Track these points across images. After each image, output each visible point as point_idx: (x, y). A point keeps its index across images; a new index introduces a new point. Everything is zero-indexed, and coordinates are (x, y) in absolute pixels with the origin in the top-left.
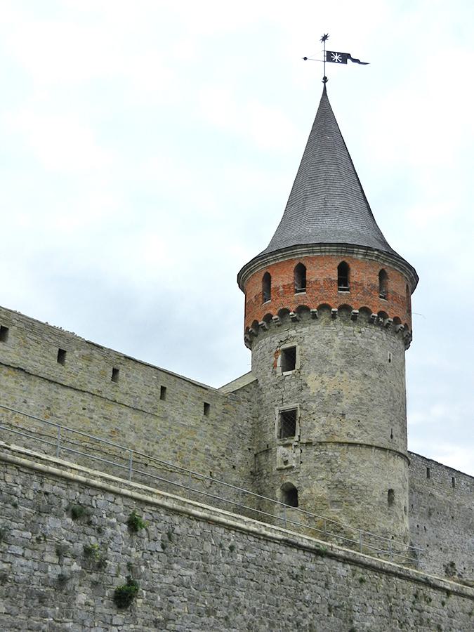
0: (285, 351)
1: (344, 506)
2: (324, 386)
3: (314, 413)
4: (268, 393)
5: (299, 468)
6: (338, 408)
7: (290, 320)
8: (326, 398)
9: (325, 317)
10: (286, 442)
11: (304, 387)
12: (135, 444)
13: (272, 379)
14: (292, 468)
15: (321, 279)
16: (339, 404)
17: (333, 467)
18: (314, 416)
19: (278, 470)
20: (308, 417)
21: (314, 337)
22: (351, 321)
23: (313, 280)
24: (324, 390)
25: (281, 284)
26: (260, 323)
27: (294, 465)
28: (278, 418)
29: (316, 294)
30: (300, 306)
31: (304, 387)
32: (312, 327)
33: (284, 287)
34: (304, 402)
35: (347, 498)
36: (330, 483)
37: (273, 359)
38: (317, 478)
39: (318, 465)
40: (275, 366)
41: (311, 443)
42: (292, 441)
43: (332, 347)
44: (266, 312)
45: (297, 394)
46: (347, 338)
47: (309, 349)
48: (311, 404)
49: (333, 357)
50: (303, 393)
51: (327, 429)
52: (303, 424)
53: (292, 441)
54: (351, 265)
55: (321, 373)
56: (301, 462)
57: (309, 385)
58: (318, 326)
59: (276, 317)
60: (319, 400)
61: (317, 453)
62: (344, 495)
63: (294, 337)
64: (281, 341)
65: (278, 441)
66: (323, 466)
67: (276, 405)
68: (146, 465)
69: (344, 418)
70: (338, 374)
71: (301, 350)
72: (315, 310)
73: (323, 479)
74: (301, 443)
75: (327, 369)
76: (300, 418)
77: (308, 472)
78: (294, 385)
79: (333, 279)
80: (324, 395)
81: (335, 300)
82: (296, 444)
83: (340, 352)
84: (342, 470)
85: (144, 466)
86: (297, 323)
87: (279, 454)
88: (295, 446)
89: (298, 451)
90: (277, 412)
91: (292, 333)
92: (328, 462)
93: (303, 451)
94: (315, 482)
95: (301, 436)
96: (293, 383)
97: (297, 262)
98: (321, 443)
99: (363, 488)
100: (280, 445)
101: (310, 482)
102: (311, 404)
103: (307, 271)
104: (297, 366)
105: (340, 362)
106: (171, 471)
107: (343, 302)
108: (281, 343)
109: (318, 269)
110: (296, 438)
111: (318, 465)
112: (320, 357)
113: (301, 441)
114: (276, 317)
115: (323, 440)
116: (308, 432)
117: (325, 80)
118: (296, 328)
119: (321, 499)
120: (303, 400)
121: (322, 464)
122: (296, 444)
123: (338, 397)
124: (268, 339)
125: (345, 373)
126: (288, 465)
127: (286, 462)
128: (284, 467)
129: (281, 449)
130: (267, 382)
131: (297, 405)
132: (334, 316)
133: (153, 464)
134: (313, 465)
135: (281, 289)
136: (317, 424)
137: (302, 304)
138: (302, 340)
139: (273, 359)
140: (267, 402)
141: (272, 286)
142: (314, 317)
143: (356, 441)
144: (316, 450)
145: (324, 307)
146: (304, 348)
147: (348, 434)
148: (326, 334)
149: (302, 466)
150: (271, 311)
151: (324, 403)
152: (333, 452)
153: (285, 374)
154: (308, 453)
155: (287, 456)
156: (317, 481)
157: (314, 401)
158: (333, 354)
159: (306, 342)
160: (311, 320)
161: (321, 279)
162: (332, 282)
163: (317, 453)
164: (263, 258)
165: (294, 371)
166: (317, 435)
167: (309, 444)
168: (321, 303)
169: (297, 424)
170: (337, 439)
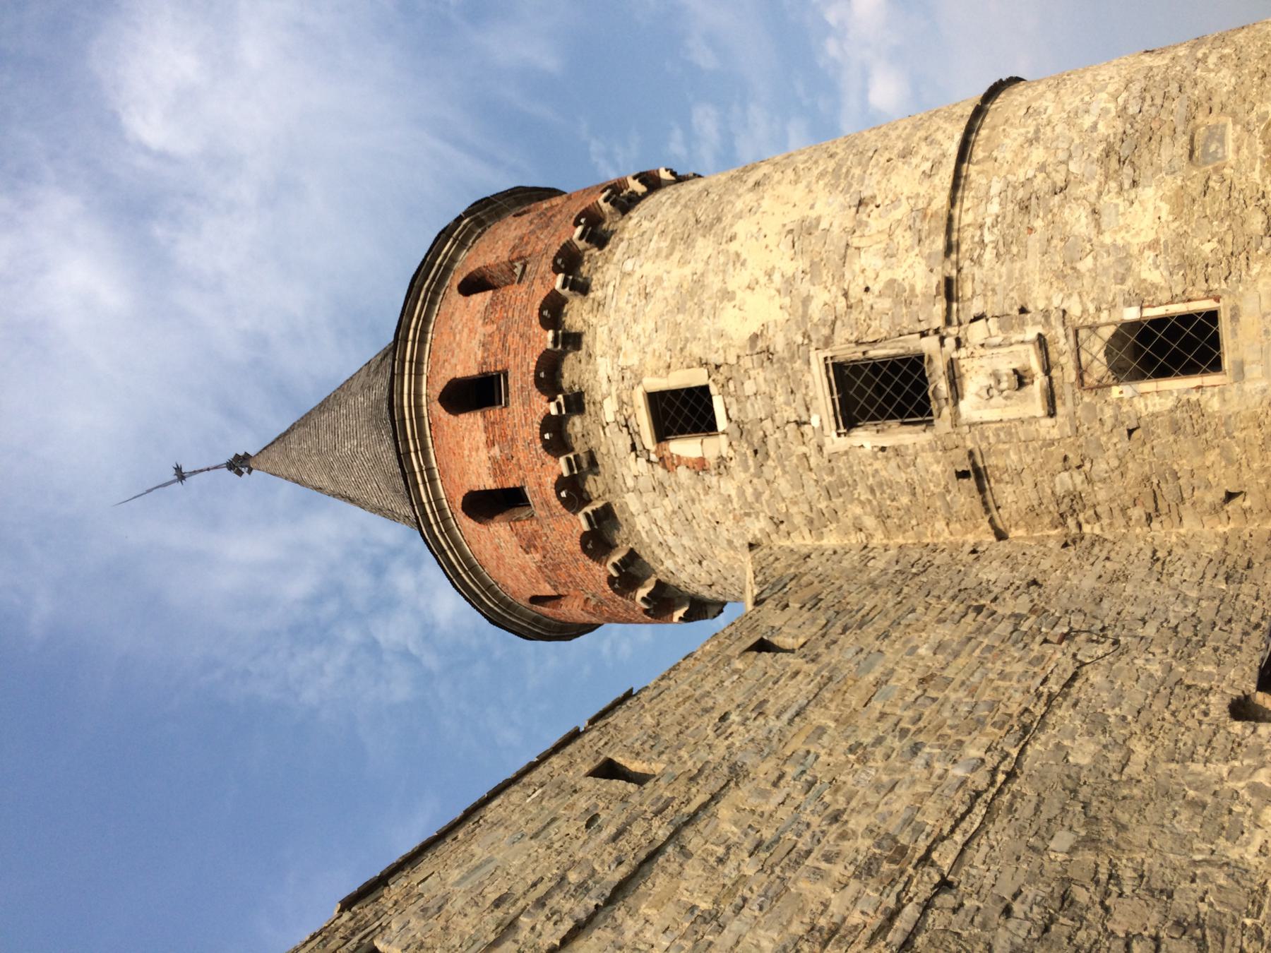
0: (662, 434)
1: (1212, 120)
2: (763, 280)
3: (846, 295)
4: (783, 485)
5: (1046, 314)
6: (836, 224)
7: (576, 420)
8: (803, 263)
9: (577, 315)
10: (943, 387)
11: (761, 344)
12: (797, 928)
13: (741, 476)
14: (1042, 342)
15: (482, 330)
16: (824, 224)
17: (1046, 187)
18: (856, 292)
19: (1052, 413)
20: (855, 314)
21: (624, 337)
22: (607, 248)
23: (480, 354)
24: (777, 277)
25: (483, 454)
26: (585, 526)
27: (1031, 333)
28: (865, 438)
29: (514, 340)
30: (538, 382)
31: (761, 344)
32: (598, 349)
33: (490, 444)
34: (806, 335)
35: (1178, 119)
36: (1113, 185)
37: (683, 473)
38: (1093, 233)
39: (1034, 242)
40: (700, 466)
41: (949, 282)
42: (939, 365)
43: (659, 280)
44: (554, 501)
45: (783, 369)
46: (643, 249)
47: (655, 345)
48: (816, 311)
49: (687, 271)
50: (779, 345)
51: (904, 239)
52: (881, 327)
53: (939, 365)
54: (472, 269)
55: (727, 295)
56: (1023, 311)
57: (755, 328)
58: (599, 330)
59: (562, 460)
60: (804, 287)
61: (989, 255)
62: (1166, 130)
63: (622, 403)
64: (634, 448)
65: (943, 424)
66: (1038, 224)
67: (820, 448)
68: (945, 885)
69: (874, 197)
70: (733, 247)
71: (655, 373)
72: (550, 334)
73: (1094, 212)
74: (948, 322)
75: (714, 282)
76: (858, 343)
77: (1066, 275)
78: (757, 380)
79: (488, 301)
80: (790, 274)
81: (537, 285)
82: (950, 342)
83: (677, 255)
84: (1062, 155)
85: (947, 900)
86: (587, 397)
87: (988, 415)
88: (959, 343)
89: (977, 332)
90: (842, 443)
91: (609, 410)
92: (1025, 208)
93: (976, 307)
94: (1107, 239)
95: (924, 326)
96: (749, 388)
97: (438, 410)
98: (950, 248)
99: (1136, 88)
100: (956, 415)
101: (1105, 260)
102: (816, 311)
103: (460, 373)
104: (697, 378)
105: (704, 246)
106: (1011, 776)
107: (546, 264)
108: (639, 447)
109: (459, 345)
110: (929, 345)
111: (1034, 242)
112: (680, 310)
113: (938, 322)
114: (562, 460)
115: (940, 243)
116: (908, 303)
117: (239, 464)
118: (599, 398)
119: (1180, 203)
120: (799, 339)
121: (1031, 230)
122: (950, 342)
123: (801, 233)
124: (632, 503)
125: (735, 229)
126: (1035, 365)
127: (1021, 379)
128: (1040, 380)
129: (970, 407)
130: (749, 491)
131: (817, 359)
132: (582, 288)
133: (945, 857)
134: (1033, 263)
135: (496, 451)
136: (885, 276)
137: (531, 378)
138: (628, 374)
139: (683, 473)
140: (812, 490)
141: (489, 483)
142: (573, 341)
143: (953, 149)
144: (977, 262)
145: (552, 312)
146: (651, 363)
147: (928, 175)
148: (622, 304)
149: (1037, 302)
150: (550, 481)
151: (813, 271)
152: (989, 200)
153: (722, 423)
154: (989, 289)
155: (996, 376)
156: (1100, 232)
157: (807, 301)
158: (674, 274)
159: (633, 360)
160: (582, 353)
161: (482, 330)
162: (493, 303)
163: (989, 255)
164: (425, 514)
165: (714, 390)
166: (921, 268)
167: (949, 289)
168: (535, 321)
169: (877, 353)
170: (942, 200)
